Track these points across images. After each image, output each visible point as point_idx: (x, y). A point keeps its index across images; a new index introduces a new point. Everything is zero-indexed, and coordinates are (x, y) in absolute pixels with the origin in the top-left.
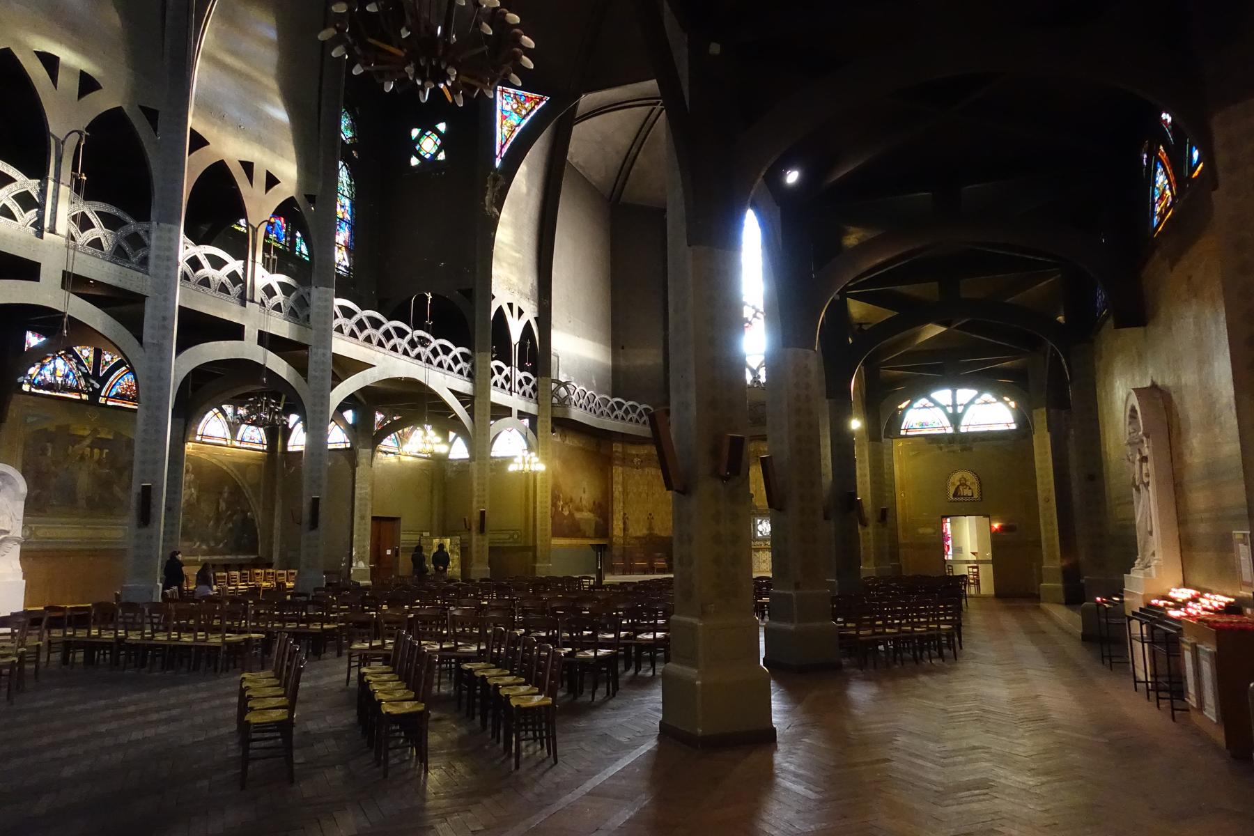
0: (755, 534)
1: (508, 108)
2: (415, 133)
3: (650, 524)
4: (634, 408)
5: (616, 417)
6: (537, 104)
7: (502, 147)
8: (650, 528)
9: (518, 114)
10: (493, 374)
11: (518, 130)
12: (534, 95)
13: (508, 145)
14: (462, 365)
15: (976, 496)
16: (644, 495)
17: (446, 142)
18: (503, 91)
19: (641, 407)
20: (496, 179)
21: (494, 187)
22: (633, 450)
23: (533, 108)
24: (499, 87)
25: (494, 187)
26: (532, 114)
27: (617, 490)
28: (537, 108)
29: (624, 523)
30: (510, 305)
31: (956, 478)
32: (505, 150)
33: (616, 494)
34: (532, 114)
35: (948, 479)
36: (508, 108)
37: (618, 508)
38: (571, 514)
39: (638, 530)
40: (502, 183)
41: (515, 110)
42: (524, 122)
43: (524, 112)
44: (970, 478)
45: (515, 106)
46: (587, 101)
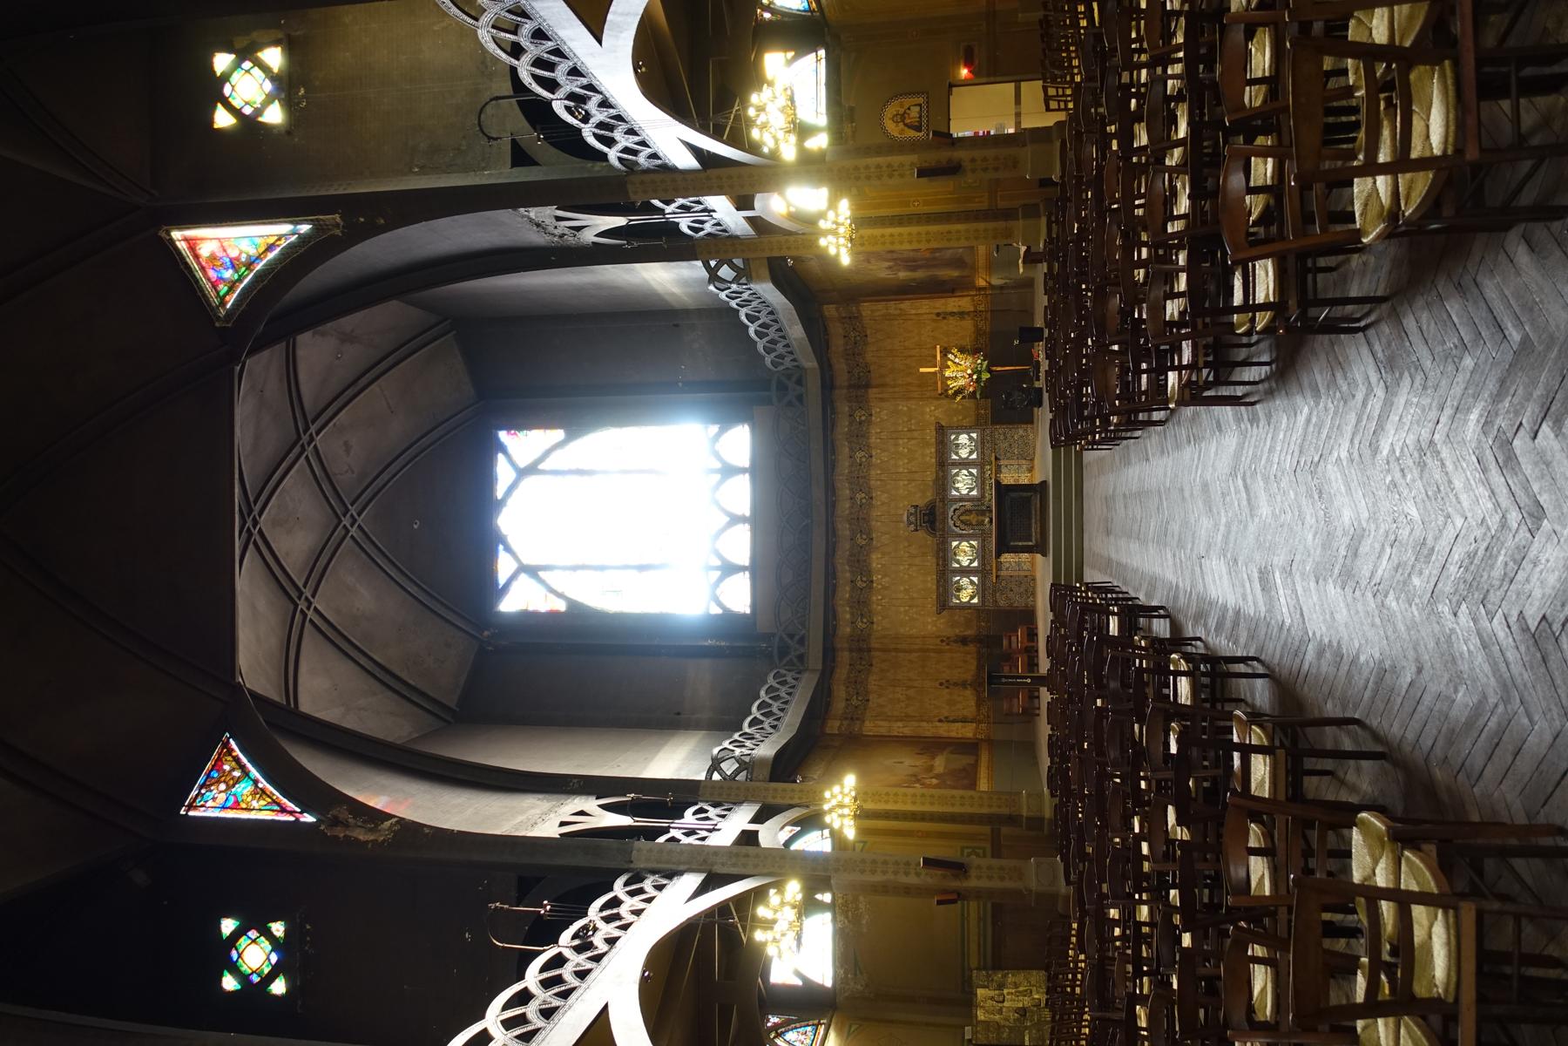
0: (971, 499)
1: (222, 796)
2: (229, 983)
3: (956, 684)
4: (770, 690)
5: (782, 710)
6: (230, 751)
7: (283, 810)
8: (964, 685)
9: (238, 781)
10: (673, 839)
11: (263, 783)
13: (284, 801)
14: (647, 885)
15: (921, 100)
16: (911, 692)
17: (255, 921)
18: (190, 807)
19: (771, 681)
20: (335, 822)
21: (346, 825)
22: (839, 706)
23: (237, 760)
24: (182, 812)
25: (346, 825)
26: (244, 760)
27: (900, 729)
28: (237, 752)
29: (954, 721)
30: (562, 824)
31: (893, 128)
32: (291, 806)
33: (907, 731)
34: (244, 760)
36: (222, 796)
37: (928, 730)
38: (937, 776)
39: (967, 702)
41: (229, 787)
42: (254, 773)
43: (237, 774)
44: (891, 110)
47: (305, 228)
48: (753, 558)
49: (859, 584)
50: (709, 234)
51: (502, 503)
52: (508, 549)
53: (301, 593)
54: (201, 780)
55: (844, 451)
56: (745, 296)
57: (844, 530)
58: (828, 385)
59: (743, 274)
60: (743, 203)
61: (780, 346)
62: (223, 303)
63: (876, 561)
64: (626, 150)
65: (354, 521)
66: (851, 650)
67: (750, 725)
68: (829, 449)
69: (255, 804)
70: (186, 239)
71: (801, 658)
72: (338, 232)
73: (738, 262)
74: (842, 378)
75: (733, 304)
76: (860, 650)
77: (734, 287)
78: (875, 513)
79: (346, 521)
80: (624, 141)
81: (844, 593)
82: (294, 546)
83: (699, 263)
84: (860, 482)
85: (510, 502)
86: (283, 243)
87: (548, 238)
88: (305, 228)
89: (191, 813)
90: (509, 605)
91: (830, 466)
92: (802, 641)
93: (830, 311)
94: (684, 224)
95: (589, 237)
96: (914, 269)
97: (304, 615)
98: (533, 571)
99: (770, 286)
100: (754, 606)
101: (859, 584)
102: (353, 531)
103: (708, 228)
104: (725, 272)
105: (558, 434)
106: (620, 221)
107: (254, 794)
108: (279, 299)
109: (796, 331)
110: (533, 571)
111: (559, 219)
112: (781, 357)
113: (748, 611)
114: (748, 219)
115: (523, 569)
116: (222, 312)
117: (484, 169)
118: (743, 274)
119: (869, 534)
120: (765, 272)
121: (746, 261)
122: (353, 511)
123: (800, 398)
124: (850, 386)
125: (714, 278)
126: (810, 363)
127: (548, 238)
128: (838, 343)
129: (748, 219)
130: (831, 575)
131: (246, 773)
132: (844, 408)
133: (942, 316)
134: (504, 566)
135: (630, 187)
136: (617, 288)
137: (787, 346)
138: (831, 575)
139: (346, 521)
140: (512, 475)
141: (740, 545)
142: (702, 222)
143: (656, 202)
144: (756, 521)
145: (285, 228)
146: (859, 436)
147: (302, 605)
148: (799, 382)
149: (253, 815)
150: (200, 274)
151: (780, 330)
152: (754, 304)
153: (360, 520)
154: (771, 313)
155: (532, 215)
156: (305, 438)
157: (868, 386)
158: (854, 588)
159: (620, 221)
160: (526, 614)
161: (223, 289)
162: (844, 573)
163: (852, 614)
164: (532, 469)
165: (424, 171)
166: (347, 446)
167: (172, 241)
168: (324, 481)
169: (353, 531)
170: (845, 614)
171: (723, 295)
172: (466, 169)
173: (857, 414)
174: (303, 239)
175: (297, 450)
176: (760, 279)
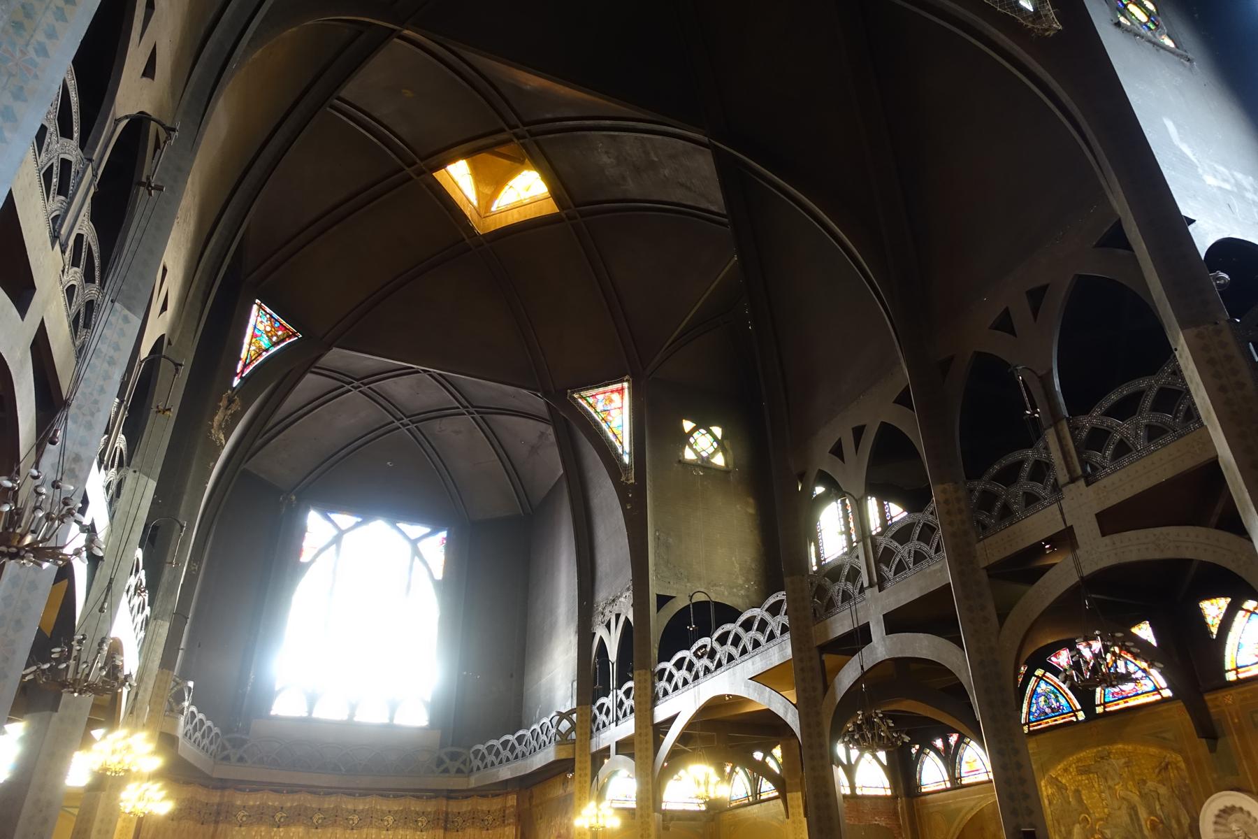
1: (261, 327)
6: (290, 337)
7: (245, 366)
9: (270, 339)
11: (265, 355)
12: (289, 326)
18: (260, 307)
19: (216, 730)
20: (231, 401)
21: (227, 408)
23: (283, 340)
25: (227, 408)
32: (247, 371)
40: (236, 407)
42: (273, 350)
43: (274, 339)
45: (268, 329)
46: (337, 357)
47: (626, 459)
48: (317, 721)
49: (279, 815)
50: (595, 717)
51: (393, 524)
52: (357, 525)
53: (365, 384)
54: (275, 315)
55: (395, 806)
56: (543, 737)
57: (329, 803)
58: (451, 795)
59: (563, 739)
60: (624, 746)
62: (582, 397)
63: (297, 831)
65: (404, 425)
66: (219, 805)
67: (192, 713)
68: (399, 793)
69: (253, 348)
70: (623, 389)
71: (227, 758)
72: (623, 479)
73: (573, 735)
74: (454, 807)
76: (218, 813)
77: (554, 731)
78: (339, 832)
79: (405, 420)
80: (679, 676)
81: (273, 800)
82: (399, 388)
83: (575, 706)
84: (368, 819)
85: (394, 532)
86: (617, 444)
87: (602, 604)
88: (626, 459)
89: (255, 307)
90: (314, 519)
91: (384, 793)
92: (241, 759)
93: (512, 800)
94: (608, 701)
95: (600, 632)
97: (349, 383)
98: (337, 540)
99: (552, 759)
100: (276, 718)
101: (279, 815)
102: (397, 423)
103: (602, 718)
104: (565, 725)
105: (439, 575)
107: (260, 348)
108: (579, 431)
110: (337, 540)
111: (618, 616)
112: (483, 758)
113: (273, 713)
114: (608, 748)
115: (341, 533)
116: (576, 396)
118: (563, 739)
119: (322, 826)
120: (563, 756)
121: (574, 742)
122: (412, 426)
123: (446, 771)
124: (447, 814)
125: (562, 716)
126: (473, 782)
127: (602, 604)
128: (484, 805)
129: (608, 748)
130: (293, 789)
131: (275, 344)
132: (431, 807)
134: (344, 520)
135: (642, 672)
136: (551, 639)
137: (493, 764)
138: (293, 789)
139: (405, 420)
140: (413, 537)
141: (331, 711)
142: (607, 714)
144: (349, 725)
145: (627, 449)
146: (406, 820)
147: (356, 384)
148: (459, 771)
149: (245, 346)
150: (601, 389)
151: (508, 760)
152: (534, 743)
153: (404, 429)
154: (524, 755)
156: (472, 410)
157: (446, 829)
158: (276, 810)
160: (303, 530)
161: (591, 400)
162: (290, 801)
163: (253, 807)
164: (416, 552)
166: (457, 433)
167: (622, 381)
168: (441, 413)
169: (397, 423)
170: (253, 800)
173: (424, 819)
174: (619, 457)
175: (466, 404)
176: (557, 752)
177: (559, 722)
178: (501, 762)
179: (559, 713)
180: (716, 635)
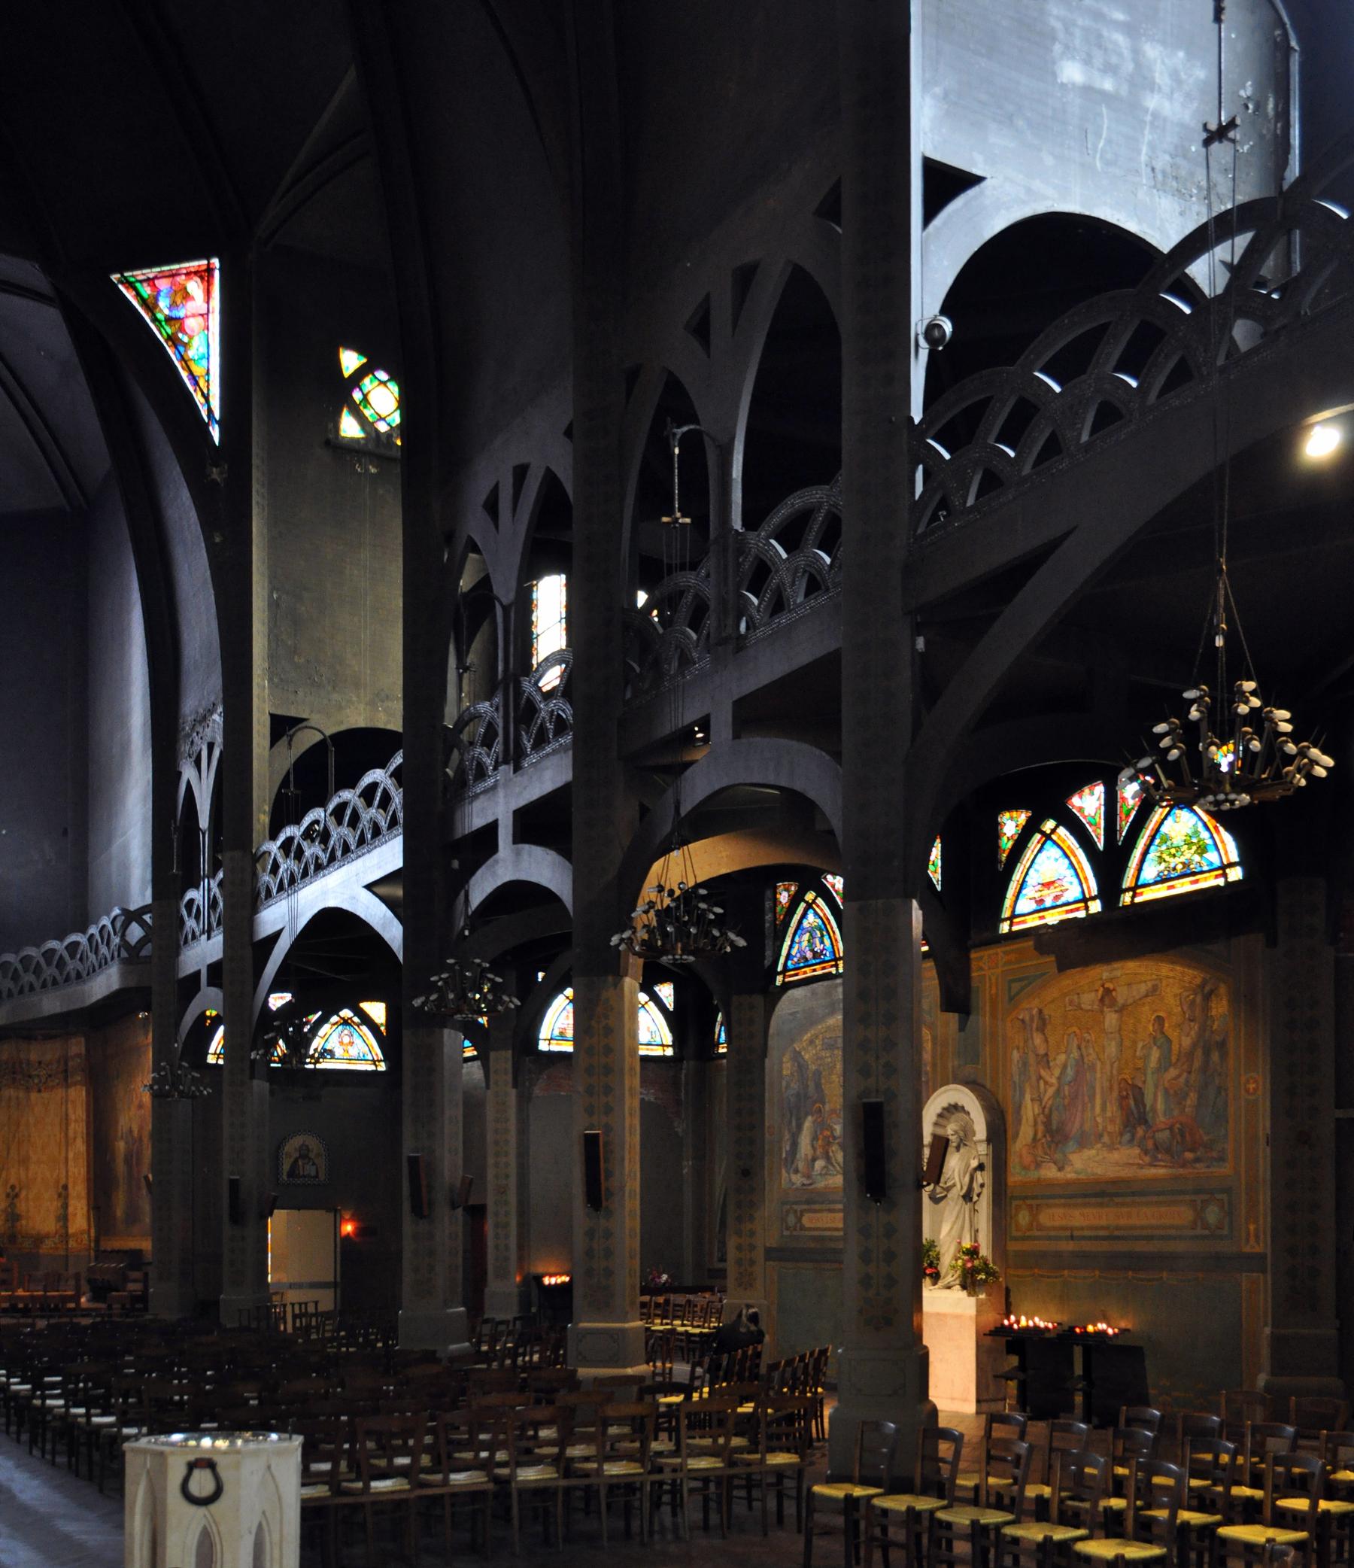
15: (322, 1176)
35: (279, 1147)
44: (313, 1143)
50: (182, 922)
56: (103, 950)
59: (131, 956)
61: (32, 978)
64: (275, 867)
73: (147, 951)
75: (93, 930)
83: (148, 900)
95: (188, 772)
96: (128, 1160)
103: (190, 923)
104: (135, 932)
106: (204, 822)
109: (51, 1004)
111: (211, 746)
117: (270, 680)
118: (131, 956)
120: (132, 983)
121: (148, 959)
129: (198, 973)
133: (64, 1193)
137: (32, 988)
143: (221, 875)
151: (55, 982)
152: (92, 957)
155: (216, 717)
159: (204, 822)
165: (273, 606)
171: (105, 921)
172: (272, 657)
176: (123, 975)
177: (125, 926)
178: (44, 985)
179: (125, 912)
180: (331, 806)
